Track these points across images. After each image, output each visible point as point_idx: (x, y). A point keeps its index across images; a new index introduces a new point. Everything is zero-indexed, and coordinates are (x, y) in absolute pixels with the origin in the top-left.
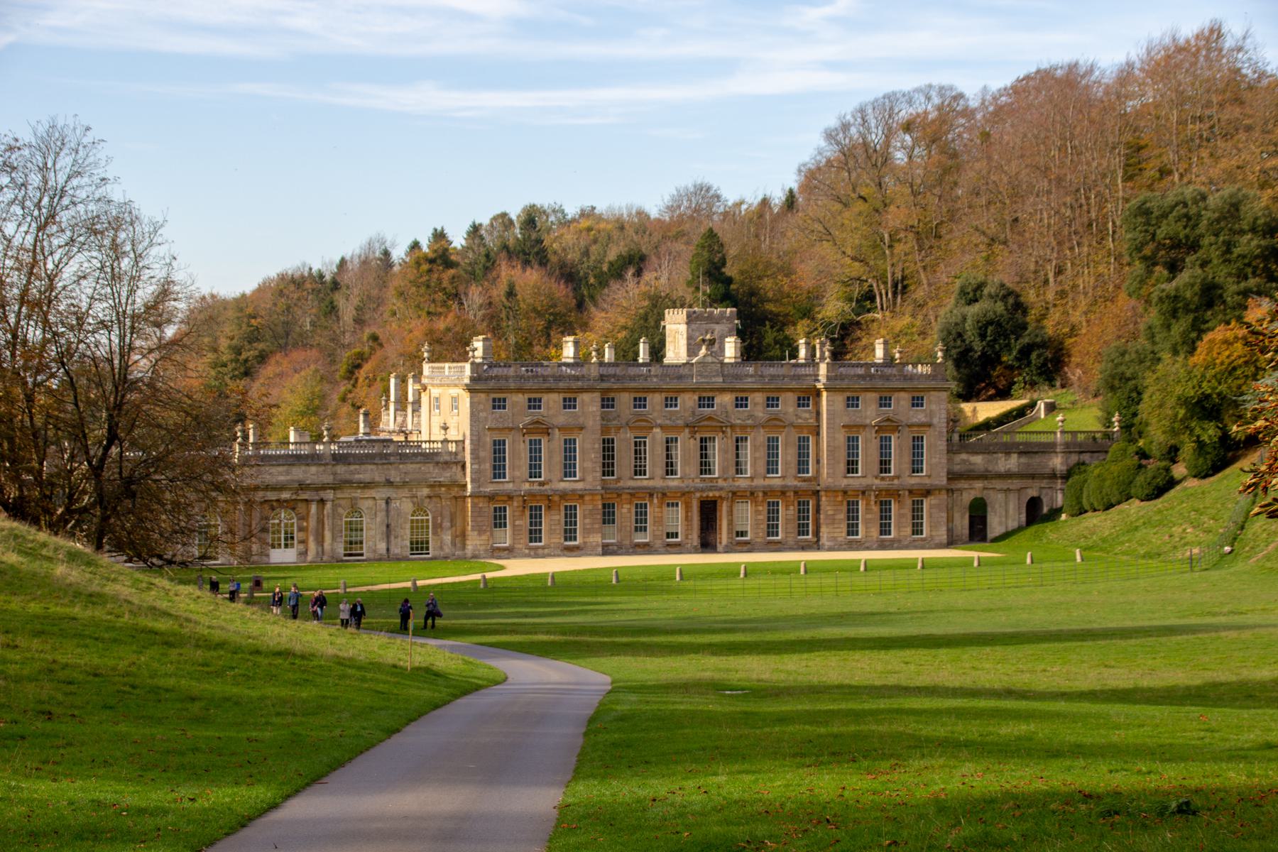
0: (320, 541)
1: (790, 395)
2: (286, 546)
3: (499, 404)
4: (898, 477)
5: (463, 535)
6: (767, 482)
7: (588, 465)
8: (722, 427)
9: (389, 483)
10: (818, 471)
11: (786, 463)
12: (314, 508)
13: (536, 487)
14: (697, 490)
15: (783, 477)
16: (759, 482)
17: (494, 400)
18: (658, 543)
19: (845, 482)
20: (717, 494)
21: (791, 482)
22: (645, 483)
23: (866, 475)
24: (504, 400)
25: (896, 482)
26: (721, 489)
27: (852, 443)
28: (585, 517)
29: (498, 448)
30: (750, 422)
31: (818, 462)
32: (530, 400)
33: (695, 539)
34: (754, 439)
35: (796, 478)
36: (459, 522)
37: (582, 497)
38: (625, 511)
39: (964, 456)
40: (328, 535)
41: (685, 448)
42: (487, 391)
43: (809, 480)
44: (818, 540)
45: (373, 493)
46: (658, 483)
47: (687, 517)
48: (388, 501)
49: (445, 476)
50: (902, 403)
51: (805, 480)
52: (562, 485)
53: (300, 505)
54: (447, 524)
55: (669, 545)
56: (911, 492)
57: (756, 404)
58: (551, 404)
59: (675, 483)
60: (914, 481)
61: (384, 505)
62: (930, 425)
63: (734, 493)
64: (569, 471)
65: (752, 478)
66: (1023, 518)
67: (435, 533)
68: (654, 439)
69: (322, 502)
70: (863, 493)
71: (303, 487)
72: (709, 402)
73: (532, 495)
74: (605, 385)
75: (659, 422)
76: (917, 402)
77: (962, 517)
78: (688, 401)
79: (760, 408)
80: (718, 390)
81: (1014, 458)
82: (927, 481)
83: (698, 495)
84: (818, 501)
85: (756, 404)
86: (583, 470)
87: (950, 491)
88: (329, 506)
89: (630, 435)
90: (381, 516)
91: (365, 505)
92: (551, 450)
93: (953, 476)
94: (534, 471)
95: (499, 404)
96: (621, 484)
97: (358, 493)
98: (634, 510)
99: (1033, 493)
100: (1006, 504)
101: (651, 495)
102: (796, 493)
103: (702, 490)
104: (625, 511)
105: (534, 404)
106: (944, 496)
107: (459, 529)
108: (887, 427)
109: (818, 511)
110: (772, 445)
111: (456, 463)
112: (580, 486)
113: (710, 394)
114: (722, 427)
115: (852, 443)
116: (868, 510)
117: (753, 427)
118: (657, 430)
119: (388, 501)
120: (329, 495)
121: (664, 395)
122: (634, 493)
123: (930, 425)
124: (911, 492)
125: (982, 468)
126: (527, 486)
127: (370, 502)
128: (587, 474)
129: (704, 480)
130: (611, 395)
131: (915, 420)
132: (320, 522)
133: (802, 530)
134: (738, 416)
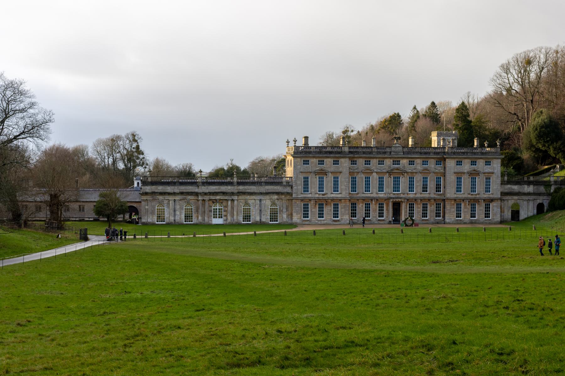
0: (232, 216)
1: (433, 160)
2: (219, 217)
3: (306, 162)
4: (479, 194)
5: (292, 214)
6: (422, 196)
7: (343, 187)
8: (403, 172)
9: (261, 194)
10: (444, 191)
11: (430, 188)
12: (229, 202)
13: (321, 196)
14: (391, 198)
15: (429, 194)
16: (418, 196)
17: (304, 161)
18: (375, 219)
19: (455, 196)
20: (400, 200)
21: (432, 196)
22: (369, 195)
23: (465, 193)
24: (308, 161)
25: (478, 196)
26: (401, 198)
27: (459, 180)
28: (342, 208)
29: (306, 180)
30: (414, 171)
31: (445, 187)
32: (319, 161)
33: (391, 218)
34: (417, 178)
35: (435, 194)
36: (290, 209)
37: (340, 200)
38: (360, 206)
39: (509, 186)
40: (235, 213)
41: (388, 181)
42: (300, 157)
43: (441, 195)
45: (254, 197)
46: (374, 195)
48: (260, 200)
50: (481, 163)
51: (439, 195)
52: (332, 195)
53: (224, 201)
54: (285, 210)
55: (379, 220)
56: (484, 200)
57: (418, 164)
58: (328, 163)
59: (382, 196)
60: (486, 196)
61: (258, 202)
62: (493, 173)
63: (408, 200)
64: (336, 189)
65: (416, 194)
66: (535, 212)
67: (280, 214)
68: (373, 177)
69: (233, 200)
70: (463, 200)
71: (224, 193)
72: (398, 163)
73: (319, 199)
74: (350, 156)
75: (375, 170)
76: (488, 163)
77: (508, 211)
78: (388, 162)
79: (419, 165)
80: (401, 158)
81: (532, 187)
82: (491, 196)
83: (392, 200)
84: (445, 203)
85: (418, 164)
86: (341, 189)
87: (501, 200)
88: (236, 202)
89: (363, 176)
90: (257, 206)
91: (251, 202)
92: (328, 181)
93: (503, 194)
94: (321, 189)
95: (306, 162)
96: (359, 195)
97: (248, 197)
98: (364, 206)
99: (539, 201)
100: (528, 205)
101: (372, 200)
102: (435, 200)
103: (393, 198)
104: (360, 206)
105: (321, 162)
106: (499, 202)
107: (290, 212)
108: (474, 174)
109: (444, 208)
110: (425, 179)
112: (340, 196)
113: (398, 160)
114: (403, 172)
115: (459, 180)
116: (465, 207)
117: (416, 173)
118: (375, 174)
119: (260, 200)
120: (235, 198)
121: (378, 160)
122: (364, 200)
123: (493, 173)
124: (484, 200)
125: (517, 191)
126: (317, 196)
127: (253, 201)
128: (344, 191)
129: (394, 194)
130: (355, 159)
131: (486, 171)
132: (232, 208)
133: (438, 215)
134: (409, 168)
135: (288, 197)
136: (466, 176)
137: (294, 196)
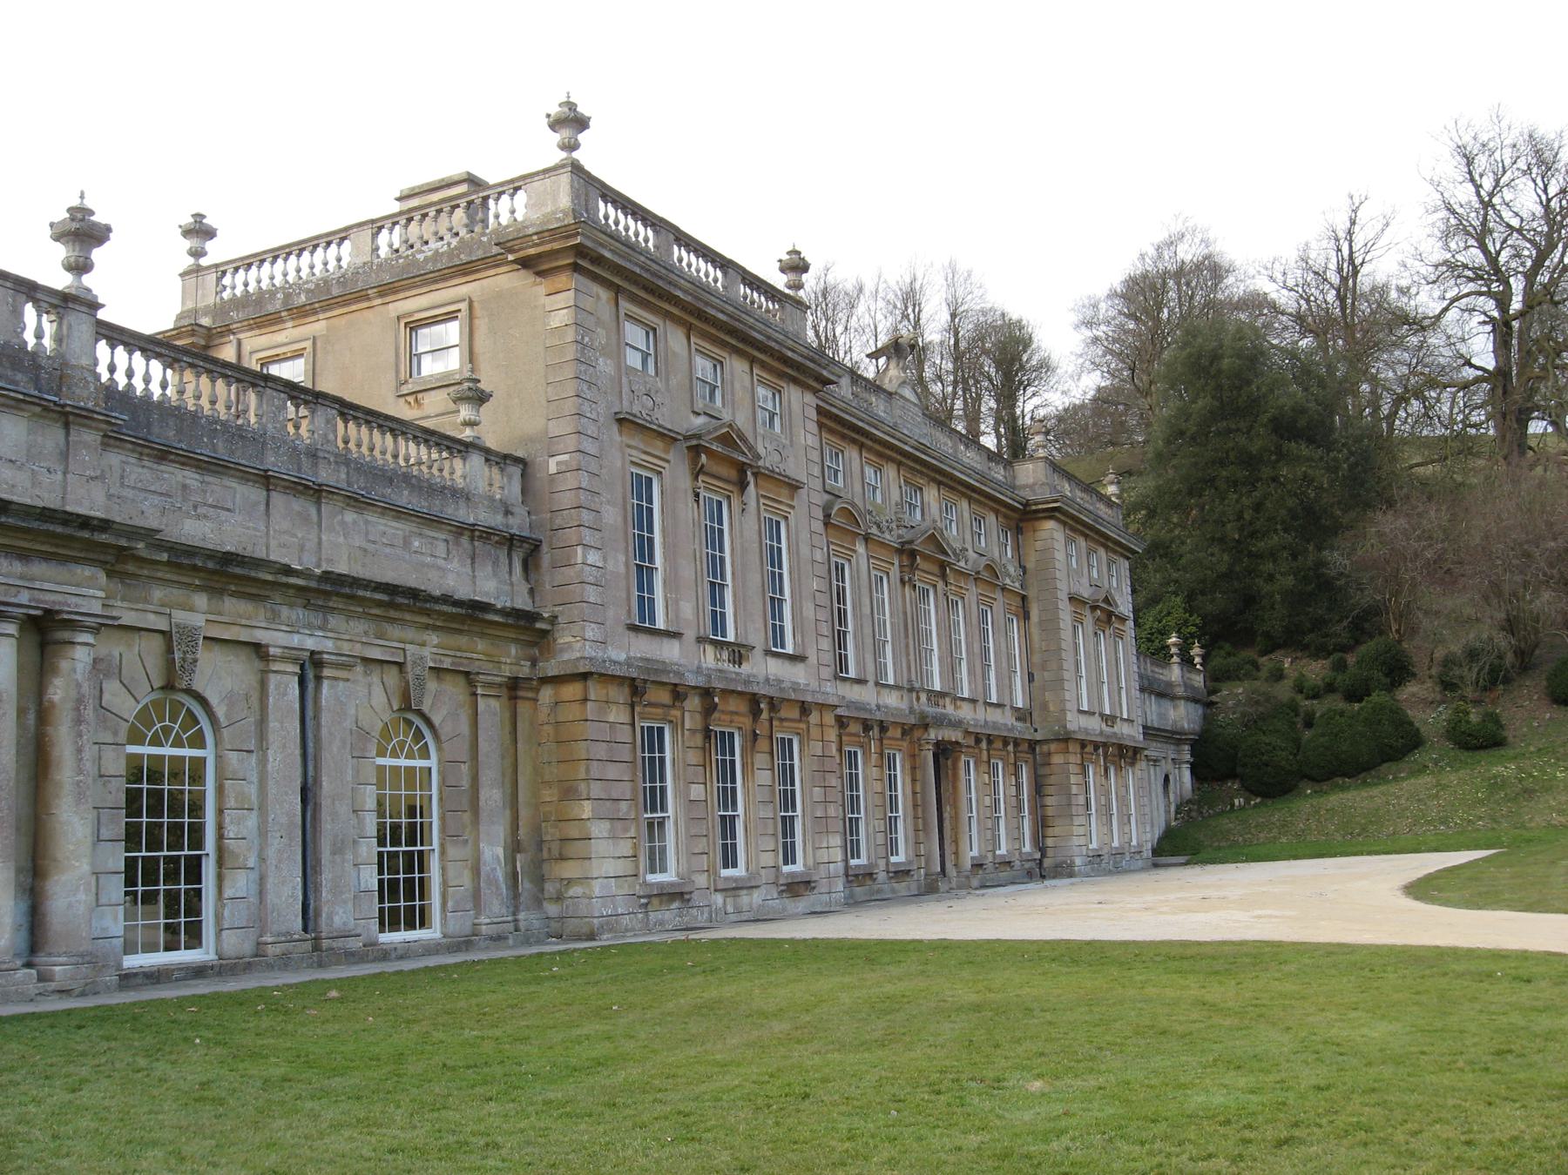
44: (1043, 856)
47: (914, 793)
48: (311, 668)
49: (493, 584)
88: (79, 658)
91: (220, 677)
97: (197, 612)
111: (511, 542)
118: (860, 548)
120: (81, 590)
135: (511, 659)
136: (1089, 620)
137: (576, 645)
